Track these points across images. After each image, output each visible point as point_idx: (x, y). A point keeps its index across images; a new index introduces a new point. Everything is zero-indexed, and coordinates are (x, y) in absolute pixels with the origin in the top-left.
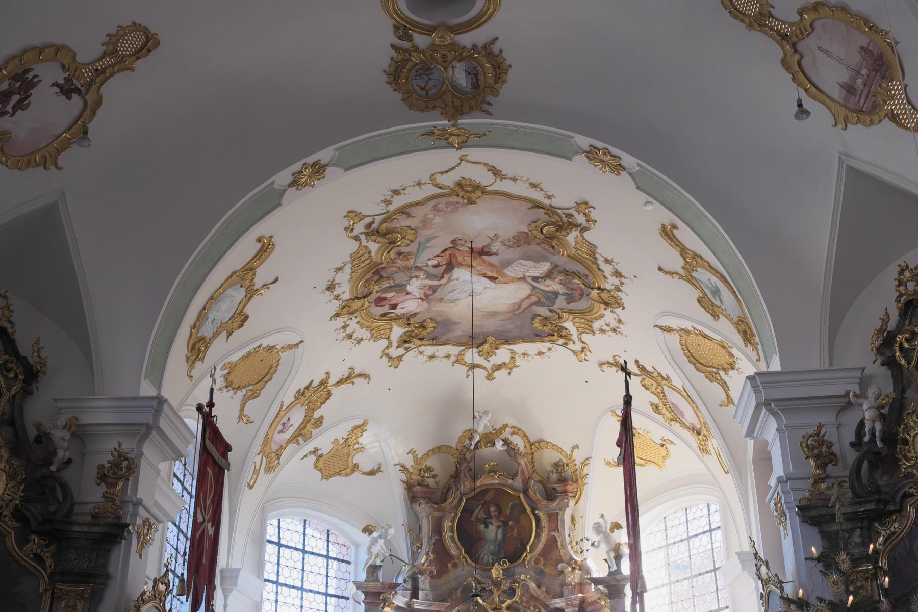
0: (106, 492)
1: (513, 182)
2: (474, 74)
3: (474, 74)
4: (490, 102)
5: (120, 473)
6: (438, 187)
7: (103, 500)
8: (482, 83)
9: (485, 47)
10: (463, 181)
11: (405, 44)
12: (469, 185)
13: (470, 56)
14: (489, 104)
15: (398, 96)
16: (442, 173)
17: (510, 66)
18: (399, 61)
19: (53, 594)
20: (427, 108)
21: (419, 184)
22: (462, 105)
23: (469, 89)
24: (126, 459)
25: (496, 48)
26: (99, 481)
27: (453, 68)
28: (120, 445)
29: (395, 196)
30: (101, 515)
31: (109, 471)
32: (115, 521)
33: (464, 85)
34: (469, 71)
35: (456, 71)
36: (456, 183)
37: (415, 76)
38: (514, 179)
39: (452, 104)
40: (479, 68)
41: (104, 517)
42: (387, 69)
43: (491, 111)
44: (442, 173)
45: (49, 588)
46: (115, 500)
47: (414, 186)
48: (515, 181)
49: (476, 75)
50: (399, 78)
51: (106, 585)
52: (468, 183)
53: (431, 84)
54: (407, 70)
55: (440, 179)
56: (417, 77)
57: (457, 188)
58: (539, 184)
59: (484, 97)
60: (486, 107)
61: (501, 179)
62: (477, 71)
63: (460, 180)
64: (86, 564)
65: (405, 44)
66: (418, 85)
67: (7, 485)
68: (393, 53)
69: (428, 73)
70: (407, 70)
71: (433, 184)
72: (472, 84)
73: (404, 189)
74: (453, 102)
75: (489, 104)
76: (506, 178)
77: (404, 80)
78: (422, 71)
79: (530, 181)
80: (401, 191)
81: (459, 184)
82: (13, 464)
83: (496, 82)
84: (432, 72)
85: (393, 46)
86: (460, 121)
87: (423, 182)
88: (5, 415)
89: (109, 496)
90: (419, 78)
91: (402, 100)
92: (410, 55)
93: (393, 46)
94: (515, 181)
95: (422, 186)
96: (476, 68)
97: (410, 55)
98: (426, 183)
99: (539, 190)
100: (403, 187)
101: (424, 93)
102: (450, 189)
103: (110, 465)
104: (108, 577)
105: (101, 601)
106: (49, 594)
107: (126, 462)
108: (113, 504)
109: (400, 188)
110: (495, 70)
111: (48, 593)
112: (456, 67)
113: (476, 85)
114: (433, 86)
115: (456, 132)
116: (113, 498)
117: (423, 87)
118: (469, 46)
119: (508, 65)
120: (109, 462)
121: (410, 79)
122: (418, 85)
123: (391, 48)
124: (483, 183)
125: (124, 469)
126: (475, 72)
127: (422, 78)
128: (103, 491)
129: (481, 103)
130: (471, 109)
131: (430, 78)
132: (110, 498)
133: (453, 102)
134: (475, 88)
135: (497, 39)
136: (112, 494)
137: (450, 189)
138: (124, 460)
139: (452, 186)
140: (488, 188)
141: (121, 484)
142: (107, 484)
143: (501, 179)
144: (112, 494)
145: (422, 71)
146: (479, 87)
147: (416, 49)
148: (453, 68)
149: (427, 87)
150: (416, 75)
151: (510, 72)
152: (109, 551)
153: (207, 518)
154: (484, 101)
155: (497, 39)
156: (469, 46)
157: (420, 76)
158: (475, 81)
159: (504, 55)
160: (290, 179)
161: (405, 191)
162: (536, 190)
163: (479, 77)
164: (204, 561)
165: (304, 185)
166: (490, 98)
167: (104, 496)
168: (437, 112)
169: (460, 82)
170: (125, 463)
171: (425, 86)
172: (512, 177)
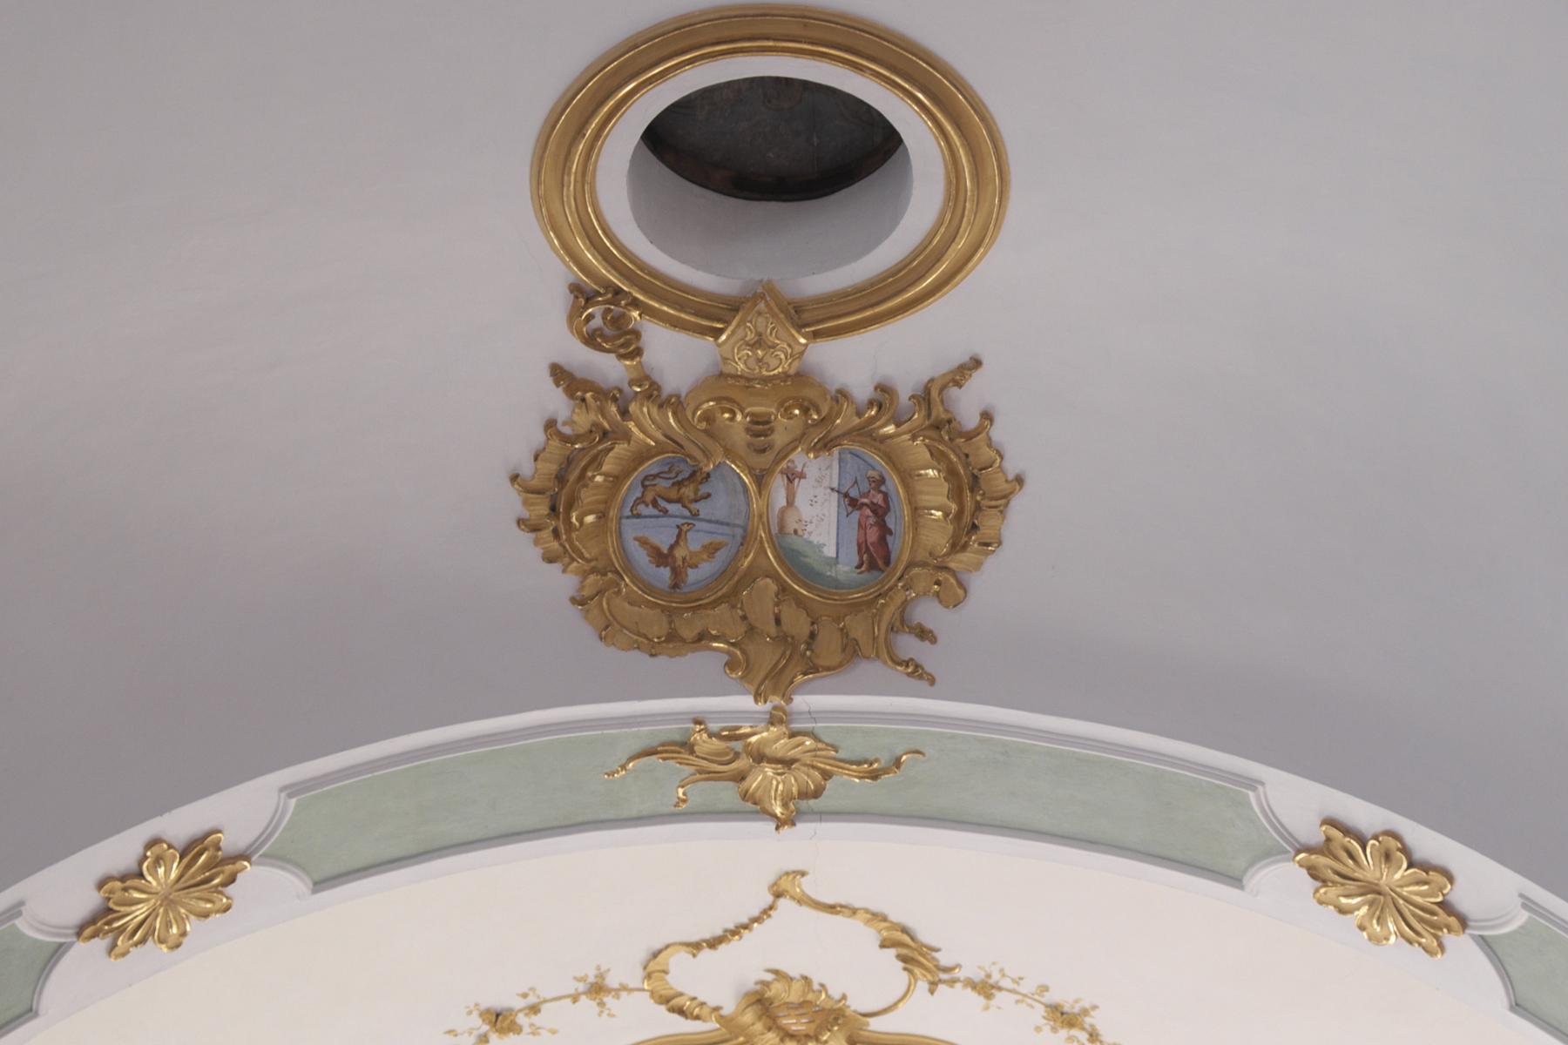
1: (981, 1000)
2: (874, 508)
3: (874, 508)
4: (929, 625)
6: (672, 1010)
8: (900, 546)
9: (924, 397)
10: (777, 989)
11: (609, 368)
12: (802, 1005)
13: (865, 434)
14: (924, 634)
15: (561, 582)
16: (695, 947)
17: (1020, 480)
18: (577, 438)
20: (673, 642)
21: (597, 989)
22: (812, 636)
23: (846, 569)
25: (966, 405)
27: (790, 481)
29: (494, 1037)
33: (830, 551)
34: (854, 493)
35: (804, 490)
36: (747, 994)
37: (636, 503)
38: (985, 988)
39: (773, 630)
40: (894, 483)
42: (527, 468)
43: (929, 667)
44: (695, 947)
47: (575, 998)
48: (989, 996)
49: (880, 512)
50: (570, 506)
52: (794, 996)
53: (695, 542)
54: (606, 475)
55: (686, 974)
56: (642, 509)
57: (748, 1017)
58: (1085, 1012)
59: (905, 604)
60: (908, 645)
61: (933, 986)
62: (886, 496)
63: (766, 984)
65: (609, 368)
66: (643, 542)
68: (557, 403)
69: (688, 491)
70: (606, 475)
71: (652, 993)
72: (862, 547)
73: (534, 1009)
74: (778, 621)
75: (924, 634)
76: (952, 982)
77: (590, 519)
78: (667, 484)
79: (1050, 998)
80: (522, 1019)
81: (760, 1001)
83: (957, 546)
84: (704, 489)
85: (559, 373)
86: (802, 702)
87: (612, 981)
90: (651, 510)
91: (574, 601)
92: (624, 413)
93: (559, 373)
94: (989, 996)
95: (608, 1000)
96: (882, 481)
97: (624, 413)
98: (624, 988)
99: (1083, 1036)
100: (532, 1000)
101: (666, 572)
102: (723, 1020)
109: (519, 1003)
110: (956, 494)
112: (802, 476)
113: (876, 555)
114: (705, 547)
115: (781, 747)
117: (665, 551)
118: (862, 390)
119: (1011, 477)
121: (613, 513)
122: (643, 542)
123: (549, 382)
124: (857, 1004)
126: (879, 499)
127: (666, 512)
129: (891, 628)
130: (852, 651)
131: (695, 515)
133: (778, 621)
134: (873, 566)
135: (976, 363)
137: (723, 1020)
139: (729, 1008)
140: (876, 1025)
143: (933, 986)
145: (667, 484)
146: (887, 562)
147: (652, 391)
148: (792, 477)
149: (680, 553)
150: (640, 500)
151: (1018, 504)
154: (903, 623)
155: (976, 363)
156: (862, 390)
157: (655, 504)
158: (873, 535)
159: (997, 433)
160: (90, 900)
161: (535, 1019)
162: (1071, 1039)
163: (890, 521)
165: (144, 933)
166: (928, 612)
168: (710, 661)
169: (815, 539)
171: (672, 548)
172: (978, 976)
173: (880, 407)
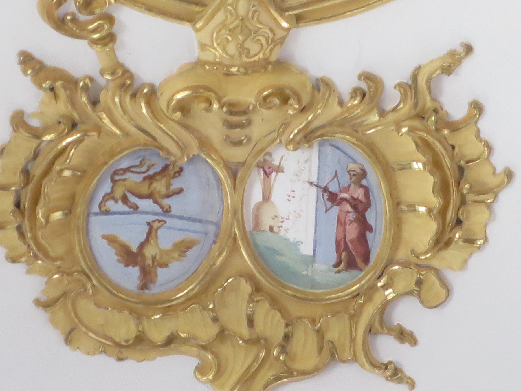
2: (355, 203)
3: (355, 203)
4: (409, 327)
17: (509, 175)
18: (46, 130)
22: (287, 337)
27: (267, 175)
33: (307, 250)
34: (334, 188)
37: (105, 199)
39: (244, 331)
43: (409, 371)
50: (36, 201)
54: (74, 169)
56: (111, 205)
59: (386, 305)
62: (367, 191)
66: (112, 240)
69: (159, 186)
70: (74, 169)
74: (251, 322)
77: (57, 215)
78: (138, 178)
84: (176, 184)
90: (120, 207)
91: (38, 303)
92: (95, 103)
96: (363, 174)
97: (95, 103)
101: (135, 272)
112: (279, 169)
114: (176, 246)
117: (134, 248)
119: (499, 169)
121: (80, 210)
122: (112, 240)
123: (18, 69)
126: (359, 194)
127: (135, 208)
129: (370, 330)
131: (167, 211)
133: (251, 322)
134: (351, 265)
145: (138, 178)
146: (366, 259)
149: (149, 252)
150: (110, 196)
157: (125, 200)
158: (352, 232)
163: (371, 216)
169: (291, 236)
171: (142, 246)
173: (364, 96)
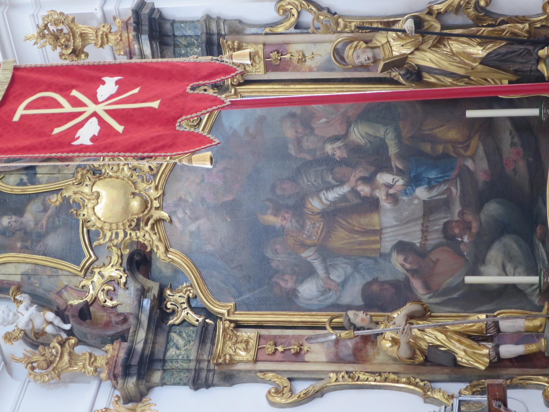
0: (96, 44)
5: (65, 31)
7: (106, 47)
19: (240, 84)
24: (46, 26)
26: (83, 56)
28: (27, 39)
30: (128, 49)
31: (67, 47)
32: (131, 28)
41: (129, 44)
45: (233, 91)
46: (104, 32)
51: (219, 18)
64: (196, 50)
67: (111, 177)
82: (82, 175)
88: (22, 180)
89: (100, 41)
103: (58, 48)
104: (208, 18)
105: (240, 22)
106: (241, 89)
107: (49, 25)
108: (110, 32)
111: (239, 90)
116: (102, 35)
120: (55, 48)
125: (59, 28)
128: (95, 48)
132: (102, 38)
136: (97, 36)
138: (49, 30)
141: (81, 28)
142: (84, 46)
144: (97, 36)
152: (173, 22)
153: (91, 107)
164: (155, 104)
167: (101, 46)
170: (52, 28)
